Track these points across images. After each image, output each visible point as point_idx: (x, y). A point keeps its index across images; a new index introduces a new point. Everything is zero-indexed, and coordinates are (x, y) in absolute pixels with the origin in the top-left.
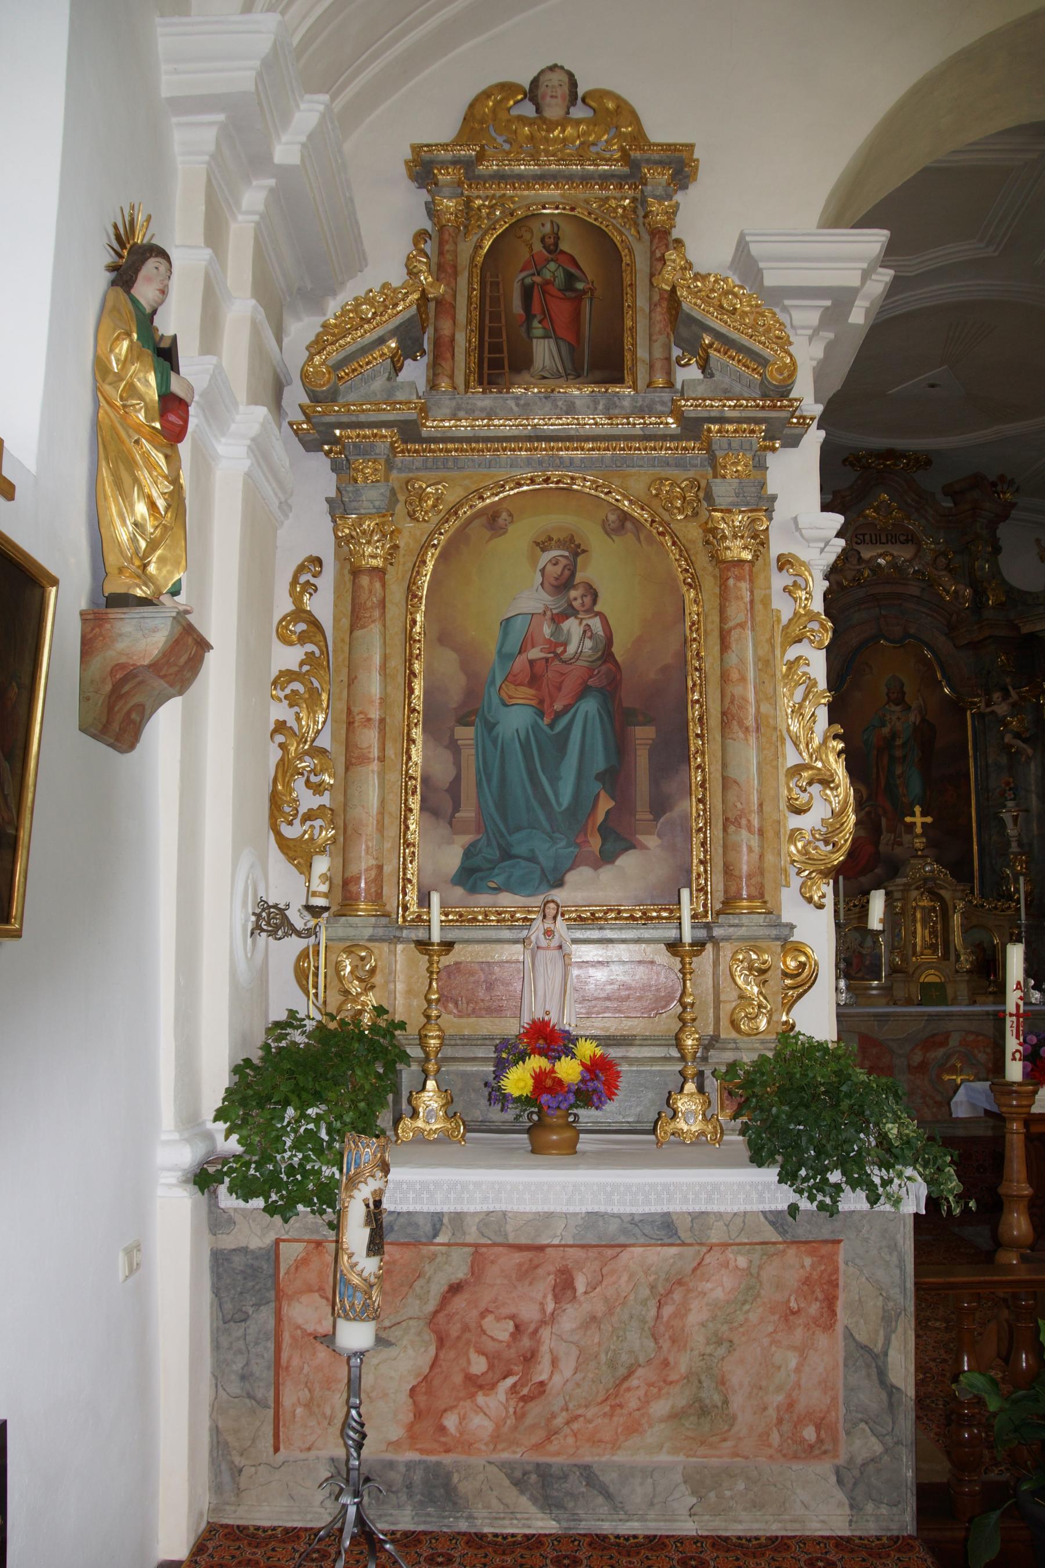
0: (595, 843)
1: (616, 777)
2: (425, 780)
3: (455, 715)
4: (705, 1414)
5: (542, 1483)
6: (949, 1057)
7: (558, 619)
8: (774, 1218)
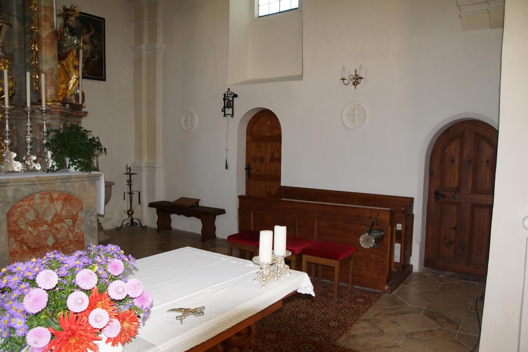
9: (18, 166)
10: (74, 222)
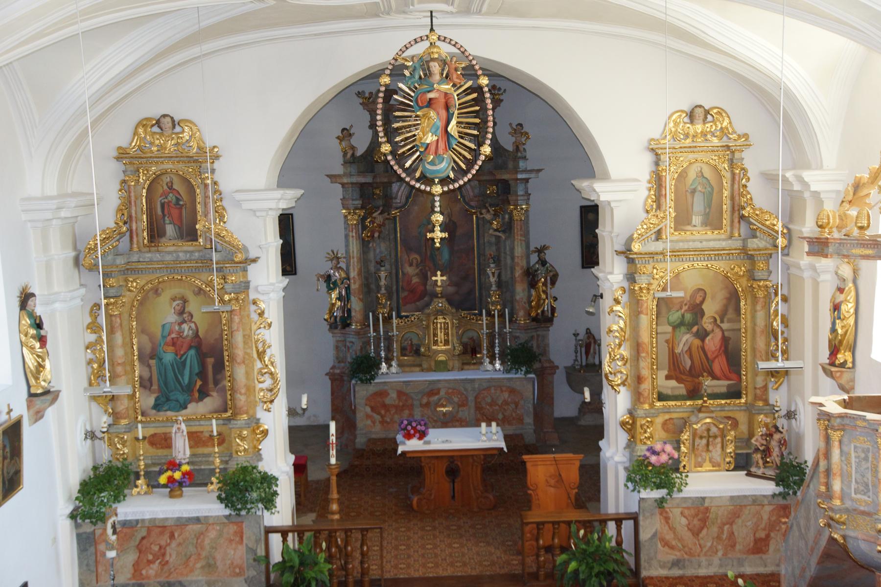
0: (197, 395)
1: (202, 374)
2: (141, 377)
3: (148, 356)
4: (210, 566)
6: (440, 400)
7: (180, 324)
8: (228, 517)
10: (516, 407)
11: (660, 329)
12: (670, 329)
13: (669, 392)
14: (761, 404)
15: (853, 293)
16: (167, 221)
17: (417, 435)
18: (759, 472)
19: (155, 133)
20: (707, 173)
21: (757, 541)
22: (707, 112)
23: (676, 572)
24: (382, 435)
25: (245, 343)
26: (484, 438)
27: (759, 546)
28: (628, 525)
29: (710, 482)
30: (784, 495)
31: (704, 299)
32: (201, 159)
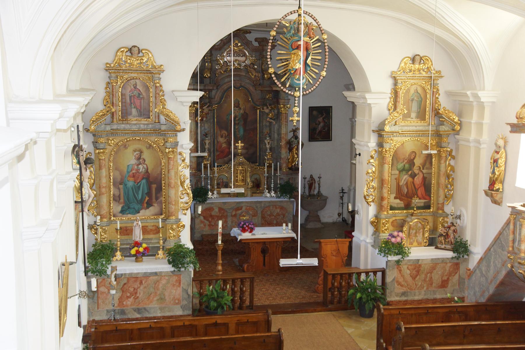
0: (145, 205)
1: (149, 194)
2: (114, 195)
3: (119, 183)
4: (162, 299)
5: (138, 311)
7: (138, 165)
8: (173, 272)
9: (268, 195)
11: (393, 172)
12: (397, 172)
13: (396, 206)
14: (440, 212)
15: (504, 155)
16: (133, 107)
17: (249, 230)
18: (443, 247)
19: (128, 56)
20: (420, 90)
21: (443, 281)
22: (421, 59)
23: (404, 298)
24: (209, 232)
25: (175, 177)
26: (284, 232)
27: (444, 284)
28: (379, 274)
29: (420, 253)
30: (458, 258)
31: (415, 157)
32: (153, 73)
